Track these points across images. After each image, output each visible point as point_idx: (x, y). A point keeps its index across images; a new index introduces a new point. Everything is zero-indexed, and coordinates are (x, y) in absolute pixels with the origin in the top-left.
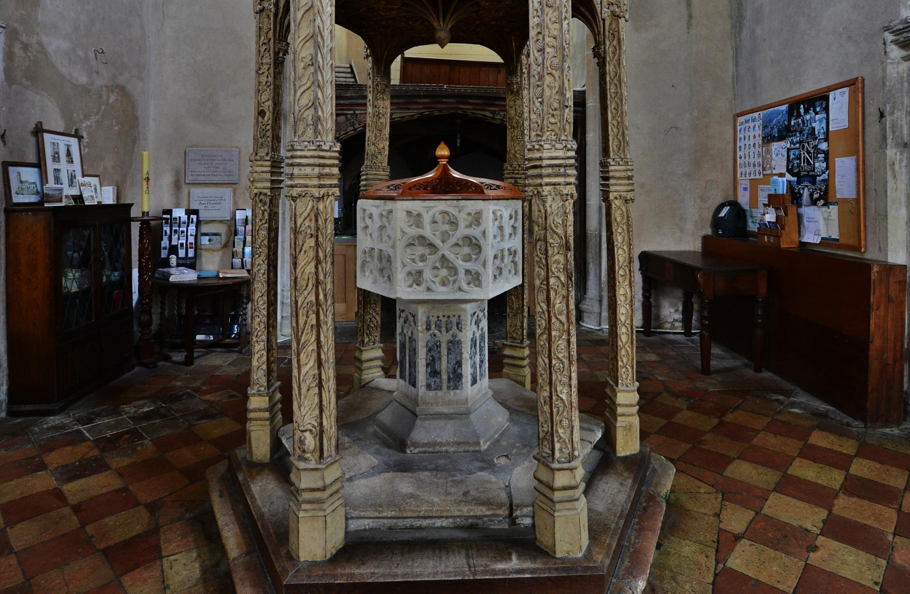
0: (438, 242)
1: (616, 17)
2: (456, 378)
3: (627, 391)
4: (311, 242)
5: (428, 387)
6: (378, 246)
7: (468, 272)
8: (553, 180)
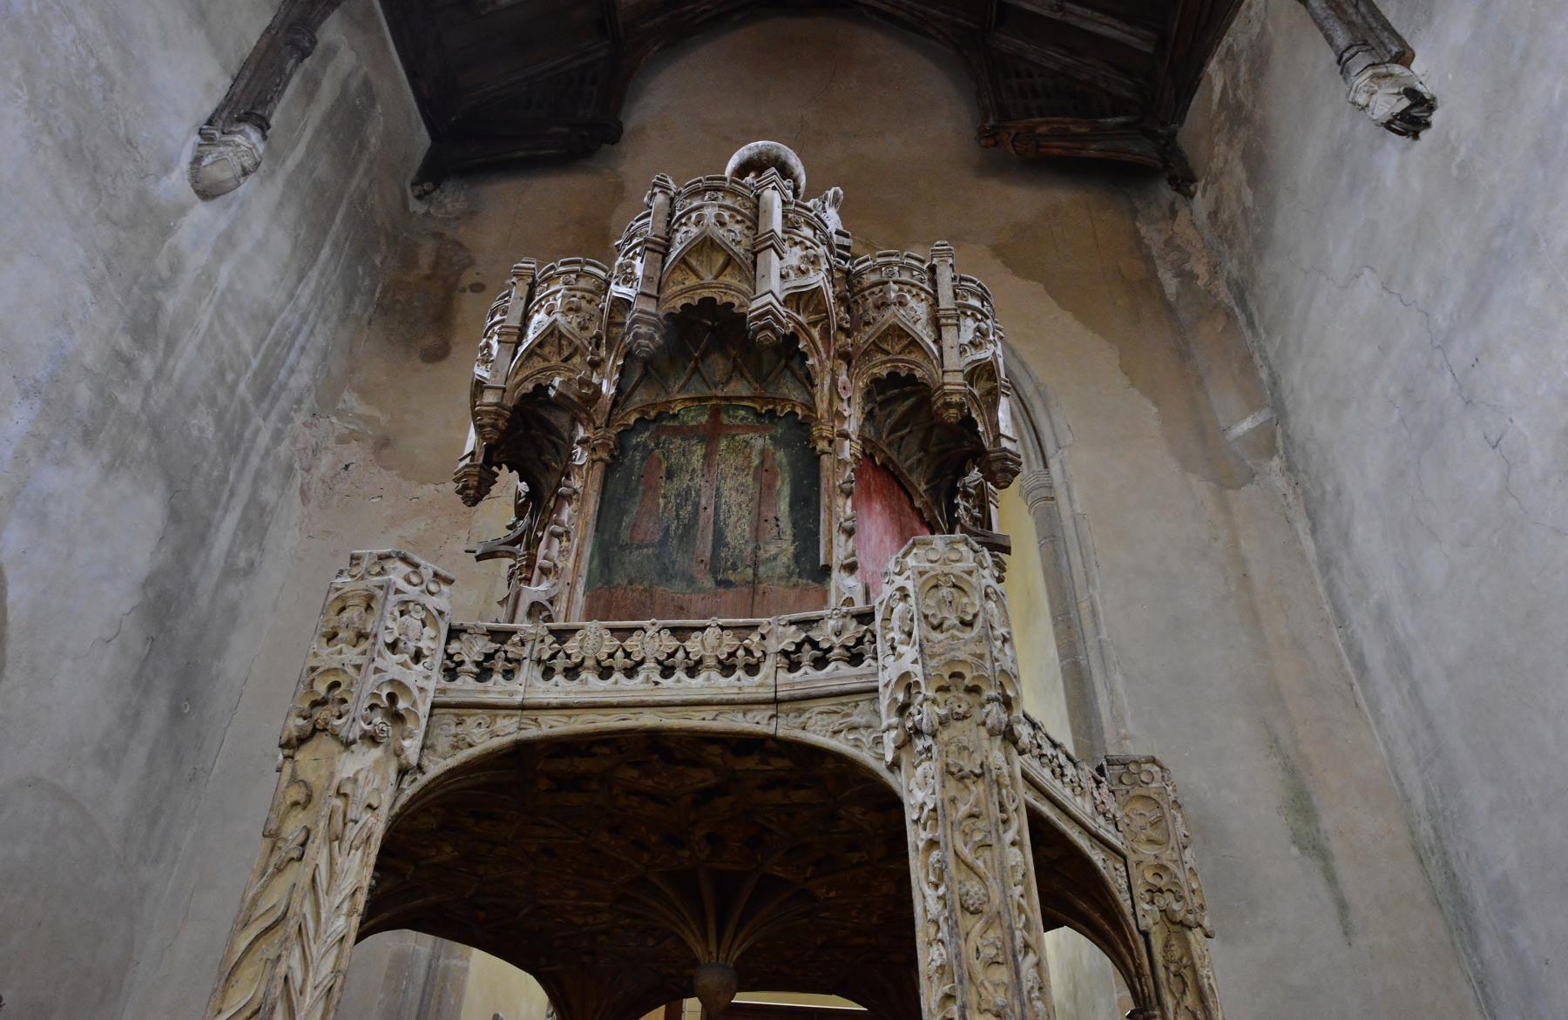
1: (1178, 926)
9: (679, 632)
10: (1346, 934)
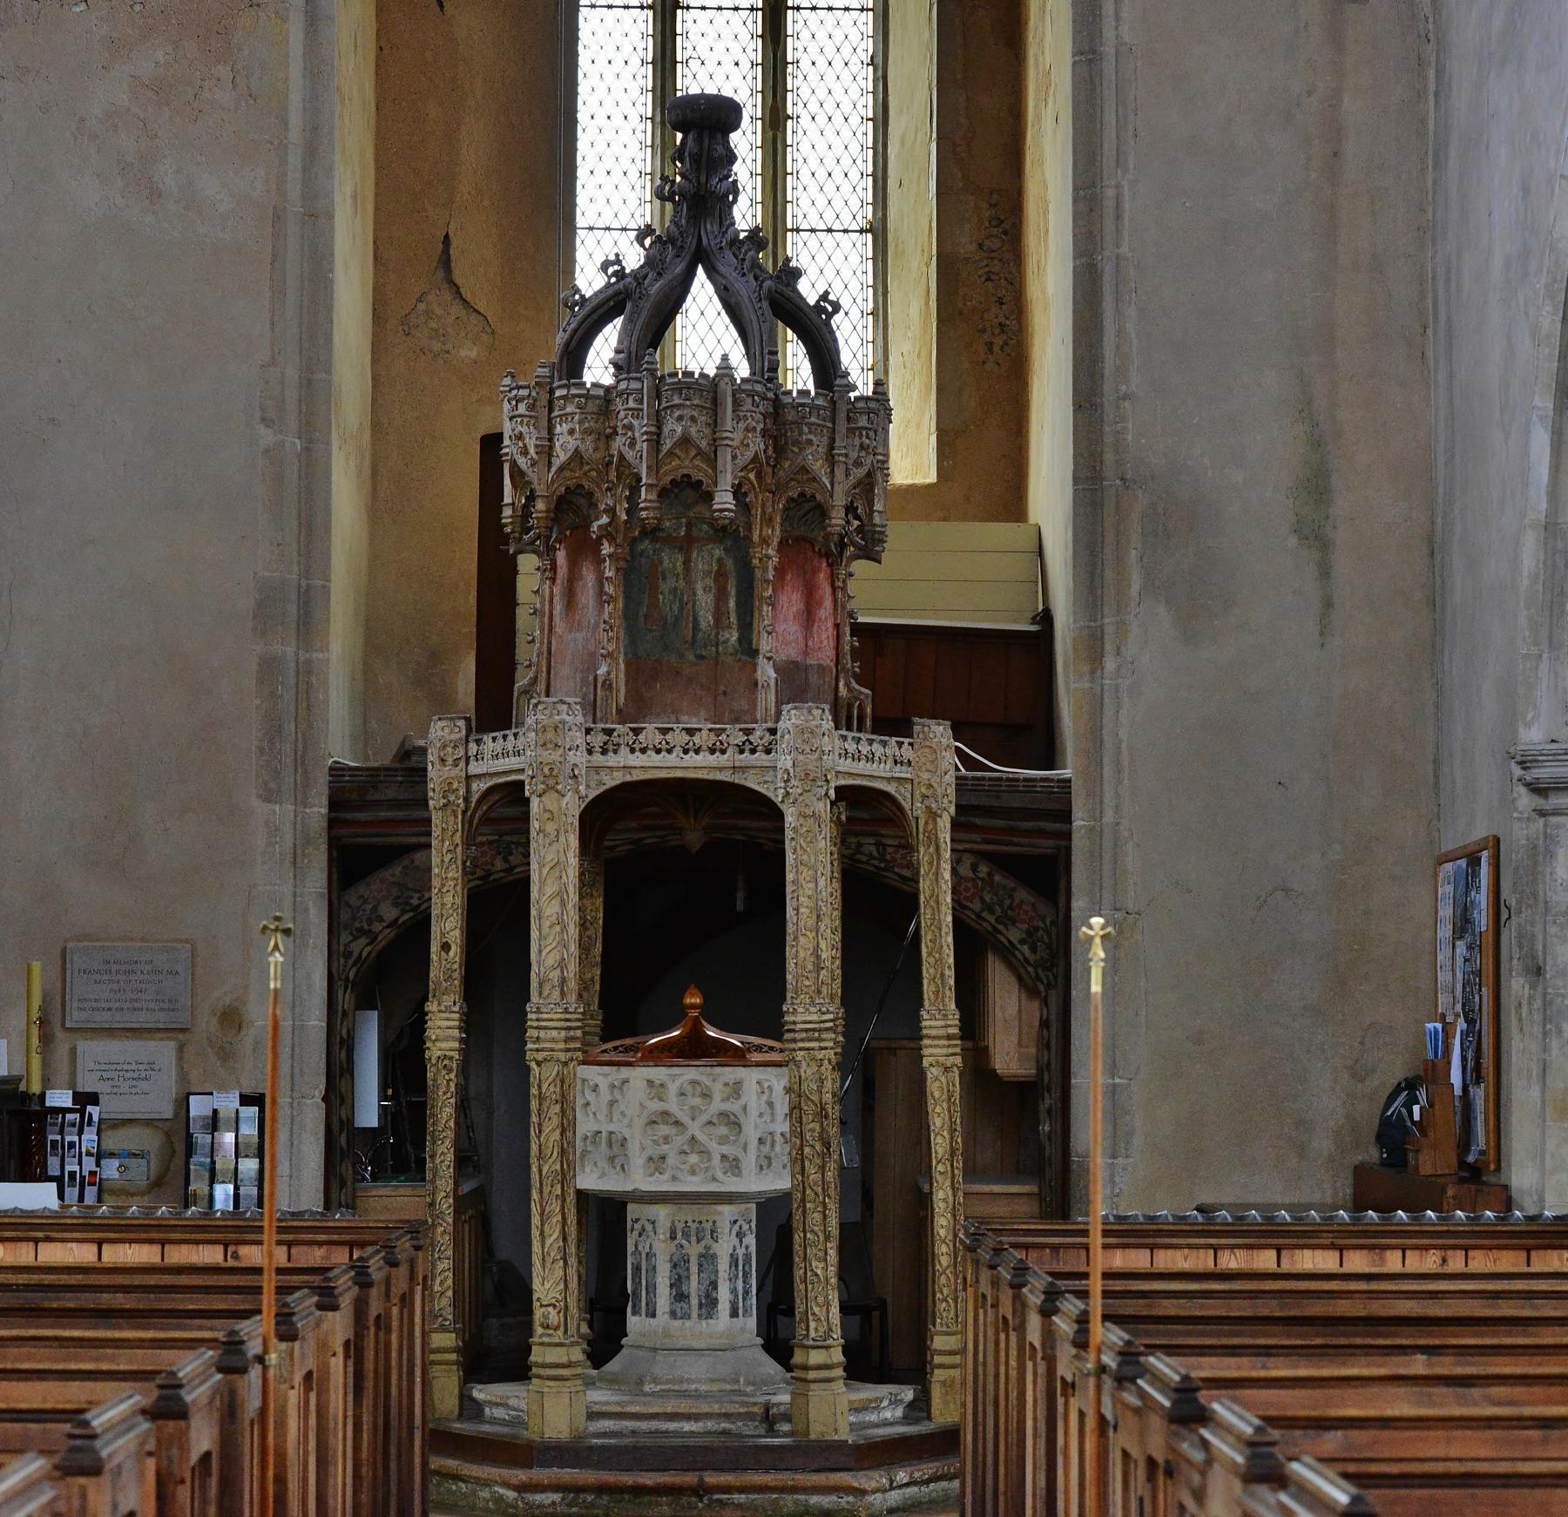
0: (686, 1120)
2: (709, 1304)
3: (948, 1334)
4: (557, 1108)
5: (673, 1314)
6: (605, 1128)
7: (724, 1157)
8: (807, 1045)
9: (691, 732)
10: (1322, 634)
